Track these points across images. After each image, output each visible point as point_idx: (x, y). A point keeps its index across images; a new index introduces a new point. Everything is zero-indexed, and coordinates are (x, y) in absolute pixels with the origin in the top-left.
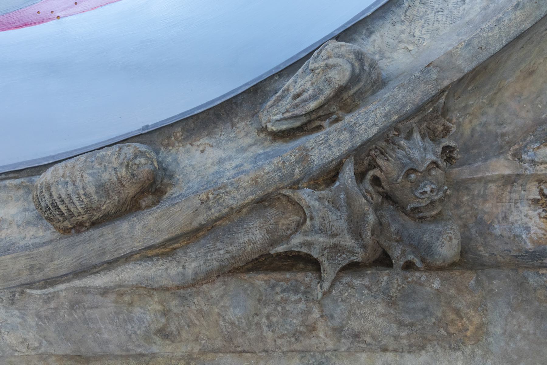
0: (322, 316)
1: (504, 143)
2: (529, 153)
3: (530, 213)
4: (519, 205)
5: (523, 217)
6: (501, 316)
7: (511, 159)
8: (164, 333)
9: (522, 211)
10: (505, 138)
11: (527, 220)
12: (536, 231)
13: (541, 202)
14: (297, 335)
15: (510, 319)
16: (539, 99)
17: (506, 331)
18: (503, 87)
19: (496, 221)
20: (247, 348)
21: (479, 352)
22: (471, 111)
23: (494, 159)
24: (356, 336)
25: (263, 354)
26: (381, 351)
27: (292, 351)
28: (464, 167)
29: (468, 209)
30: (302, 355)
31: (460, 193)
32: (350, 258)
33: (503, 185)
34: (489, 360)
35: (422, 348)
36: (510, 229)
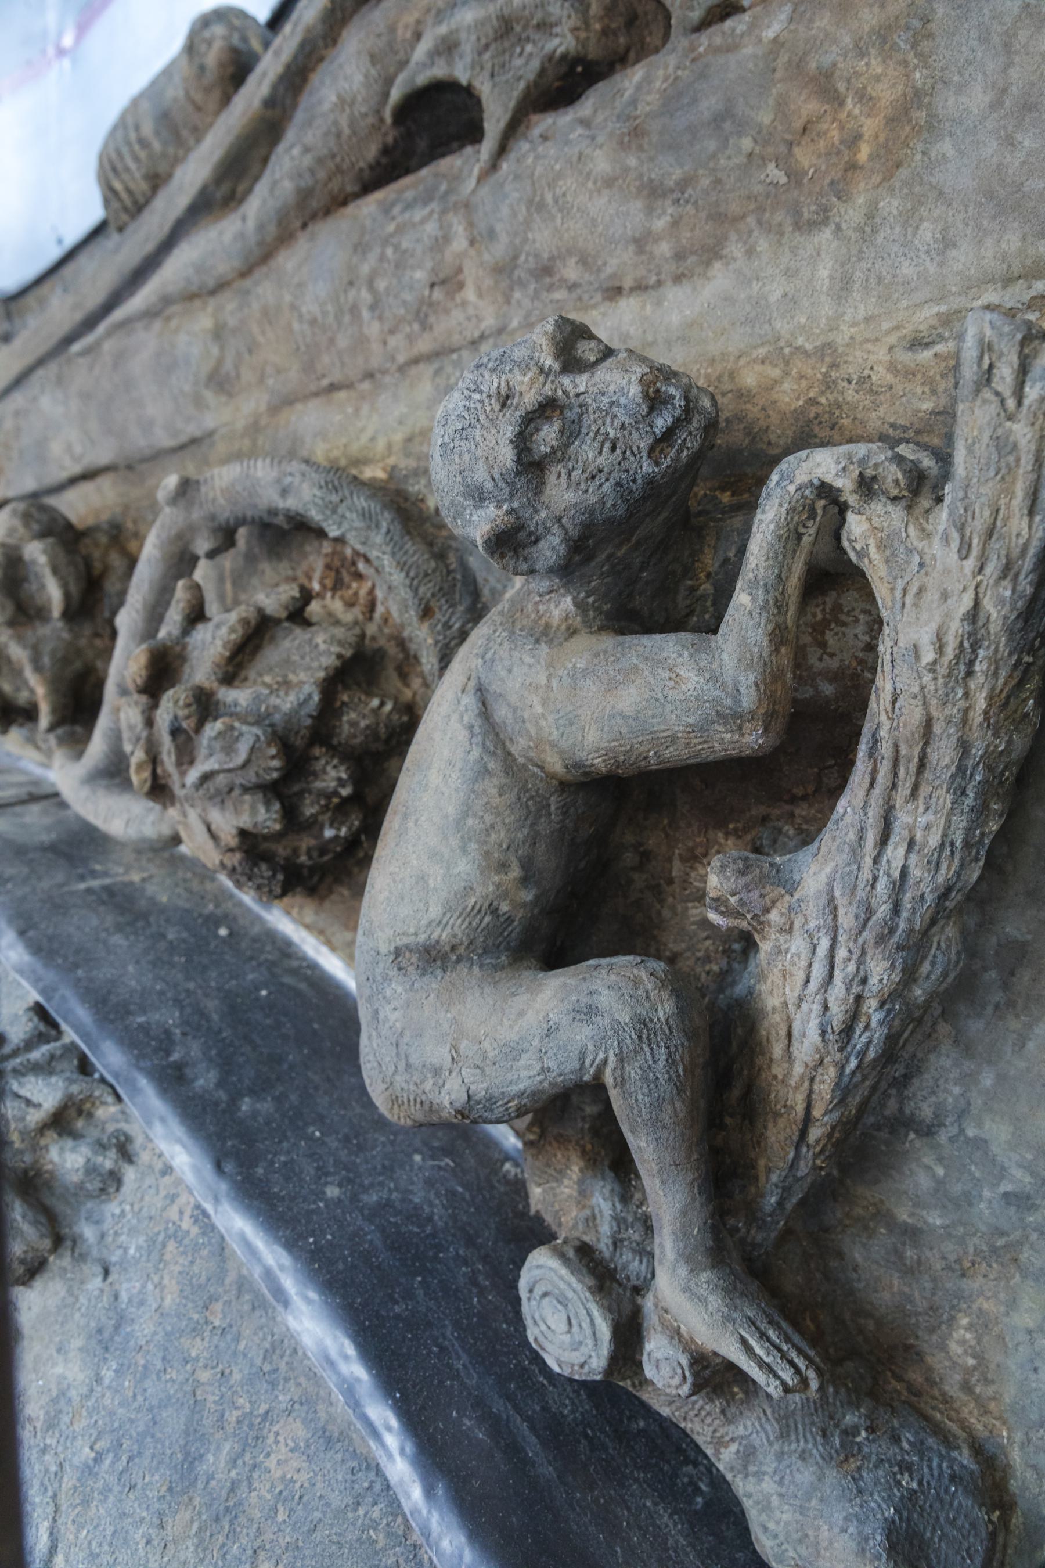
0: (472, 243)
6: (985, 39)
8: (220, 382)
14: (423, 315)
15: (1023, 36)
17: (1004, 91)
20: (336, 376)
21: (891, 205)
24: (545, 271)
25: (366, 386)
26: (604, 299)
27: (416, 361)
30: (436, 365)
32: (543, 48)
34: (925, 224)
35: (711, 253)
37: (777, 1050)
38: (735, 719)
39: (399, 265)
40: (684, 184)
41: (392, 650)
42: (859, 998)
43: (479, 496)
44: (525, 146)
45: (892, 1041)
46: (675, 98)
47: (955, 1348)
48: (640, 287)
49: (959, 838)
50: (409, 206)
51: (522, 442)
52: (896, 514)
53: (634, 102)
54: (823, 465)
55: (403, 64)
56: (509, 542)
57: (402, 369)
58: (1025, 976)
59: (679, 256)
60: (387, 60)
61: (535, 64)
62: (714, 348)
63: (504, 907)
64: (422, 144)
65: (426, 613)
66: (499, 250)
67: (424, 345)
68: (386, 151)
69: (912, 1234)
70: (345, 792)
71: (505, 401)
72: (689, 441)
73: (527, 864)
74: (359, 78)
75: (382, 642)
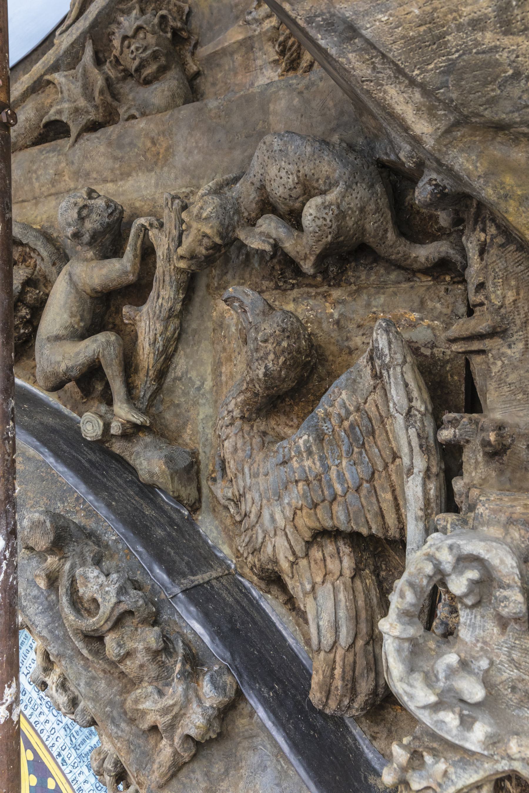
6: (182, 137)
35: (129, 175)
37: (141, 353)
38: (126, 273)
39: (46, 167)
40: (122, 158)
41: (41, 279)
42: (156, 334)
43: (69, 225)
44: (82, 141)
45: (165, 347)
46: (120, 136)
47: (188, 431)
48: (112, 181)
49: (172, 296)
50: (47, 152)
51: (79, 213)
52: (157, 231)
53: (110, 135)
54: (142, 221)
55: (47, 113)
56: (77, 235)
57: (45, 197)
58: (197, 336)
59: (121, 174)
60: (41, 111)
61: (85, 121)
62: (130, 197)
63: (76, 326)
64: (51, 134)
65: (54, 264)
66: (74, 168)
67: (53, 191)
68: (40, 134)
69: (178, 406)
70: (28, 317)
71: (75, 204)
72: (116, 215)
73: (82, 316)
74: (32, 114)
75: (39, 277)
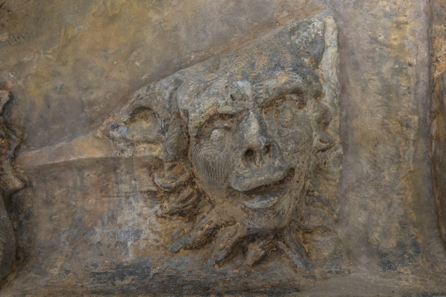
1: (94, 115)
2: (120, 128)
3: (146, 211)
4: (131, 199)
5: (136, 216)
7: (100, 136)
9: (136, 207)
10: (95, 107)
11: (141, 220)
12: (149, 235)
13: (159, 195)
16: (135, 53)
18: (73, 37)
19: (100, 222)
22: (33, 72)
23: (82, 137)
28: (43, 149)
29: (63, 206)
31: (48, 184)
33: (105, 173)
36: (114, 233)
